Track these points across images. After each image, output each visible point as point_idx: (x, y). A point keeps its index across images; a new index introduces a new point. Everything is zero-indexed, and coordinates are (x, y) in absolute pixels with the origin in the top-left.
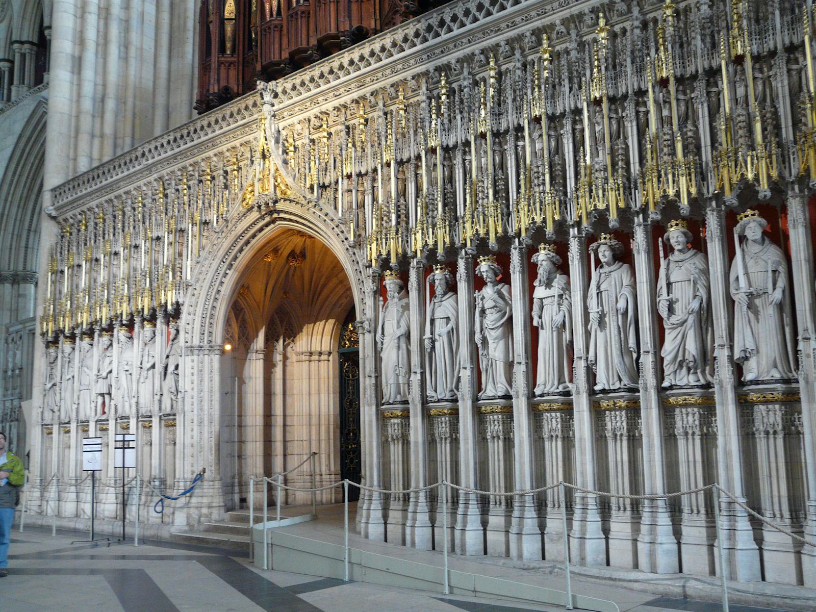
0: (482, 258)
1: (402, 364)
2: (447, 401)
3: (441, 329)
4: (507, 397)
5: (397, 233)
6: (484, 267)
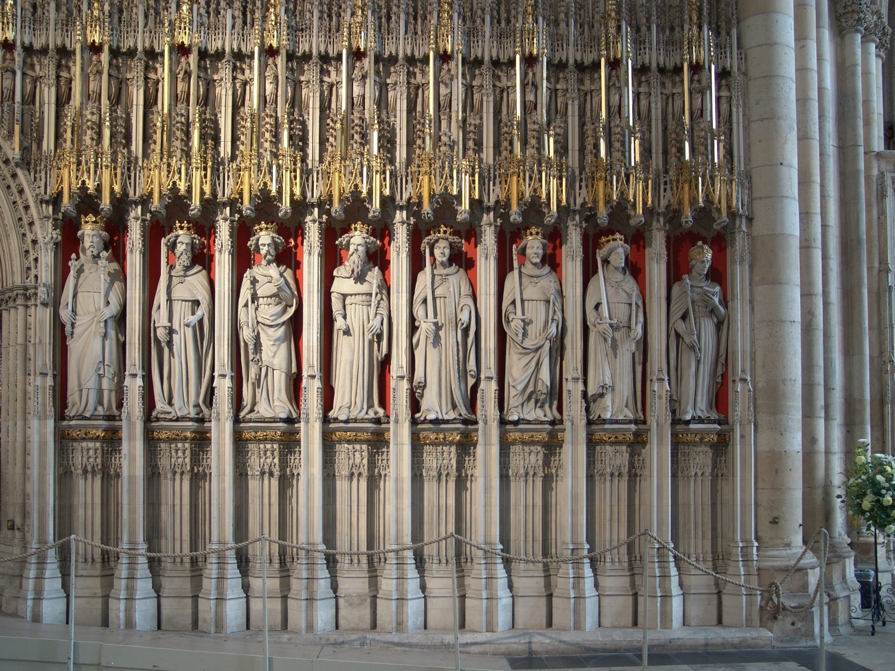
0: (263, 225)
1: (110, 360)
2: (191, 420)
3: (183, 316)
4: (290, 420)
5: (114, 160)
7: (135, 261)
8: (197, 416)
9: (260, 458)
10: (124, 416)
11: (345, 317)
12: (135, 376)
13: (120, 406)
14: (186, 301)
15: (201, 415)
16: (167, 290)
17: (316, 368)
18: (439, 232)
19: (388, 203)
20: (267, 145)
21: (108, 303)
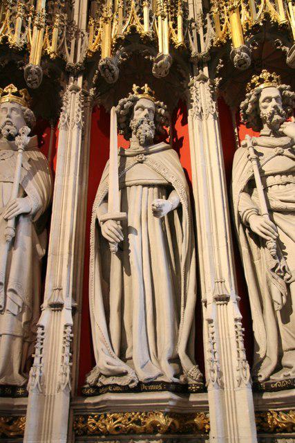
0: (265, 74)
2: (166, 386)
8: (176, 380)
12: (57, 307)
14: (149, 186)
15: (182, 379)
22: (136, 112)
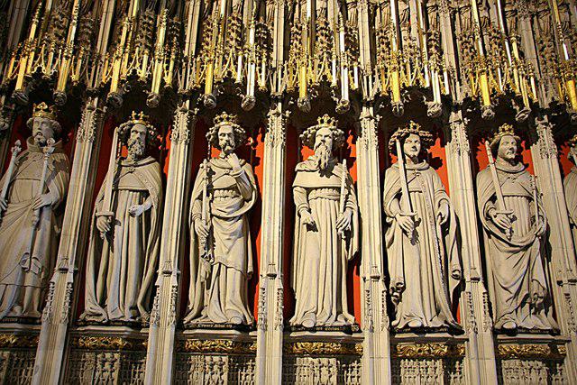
0: (225, 115)
1: (39, 252)
2: (125, 324)
4: (243, 327)
5: (76, 52)
6: (225, 128)
7: (83, 150)
8: (132, 320)
9: (205, 374)
10: (45, 317)
11: (310, 211)
12: (64, 271)
13: (42, 306)
14: (134, 191)
16: (114, 180)
17: (276, 266)
18: (409, 127)
19: (356, 96)
20: (233, 43)
21: (48, 191)
22: (132, 134)
